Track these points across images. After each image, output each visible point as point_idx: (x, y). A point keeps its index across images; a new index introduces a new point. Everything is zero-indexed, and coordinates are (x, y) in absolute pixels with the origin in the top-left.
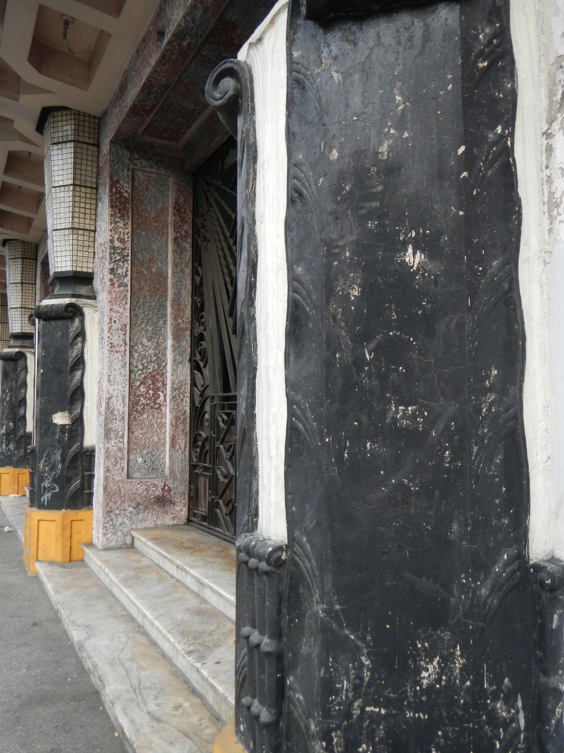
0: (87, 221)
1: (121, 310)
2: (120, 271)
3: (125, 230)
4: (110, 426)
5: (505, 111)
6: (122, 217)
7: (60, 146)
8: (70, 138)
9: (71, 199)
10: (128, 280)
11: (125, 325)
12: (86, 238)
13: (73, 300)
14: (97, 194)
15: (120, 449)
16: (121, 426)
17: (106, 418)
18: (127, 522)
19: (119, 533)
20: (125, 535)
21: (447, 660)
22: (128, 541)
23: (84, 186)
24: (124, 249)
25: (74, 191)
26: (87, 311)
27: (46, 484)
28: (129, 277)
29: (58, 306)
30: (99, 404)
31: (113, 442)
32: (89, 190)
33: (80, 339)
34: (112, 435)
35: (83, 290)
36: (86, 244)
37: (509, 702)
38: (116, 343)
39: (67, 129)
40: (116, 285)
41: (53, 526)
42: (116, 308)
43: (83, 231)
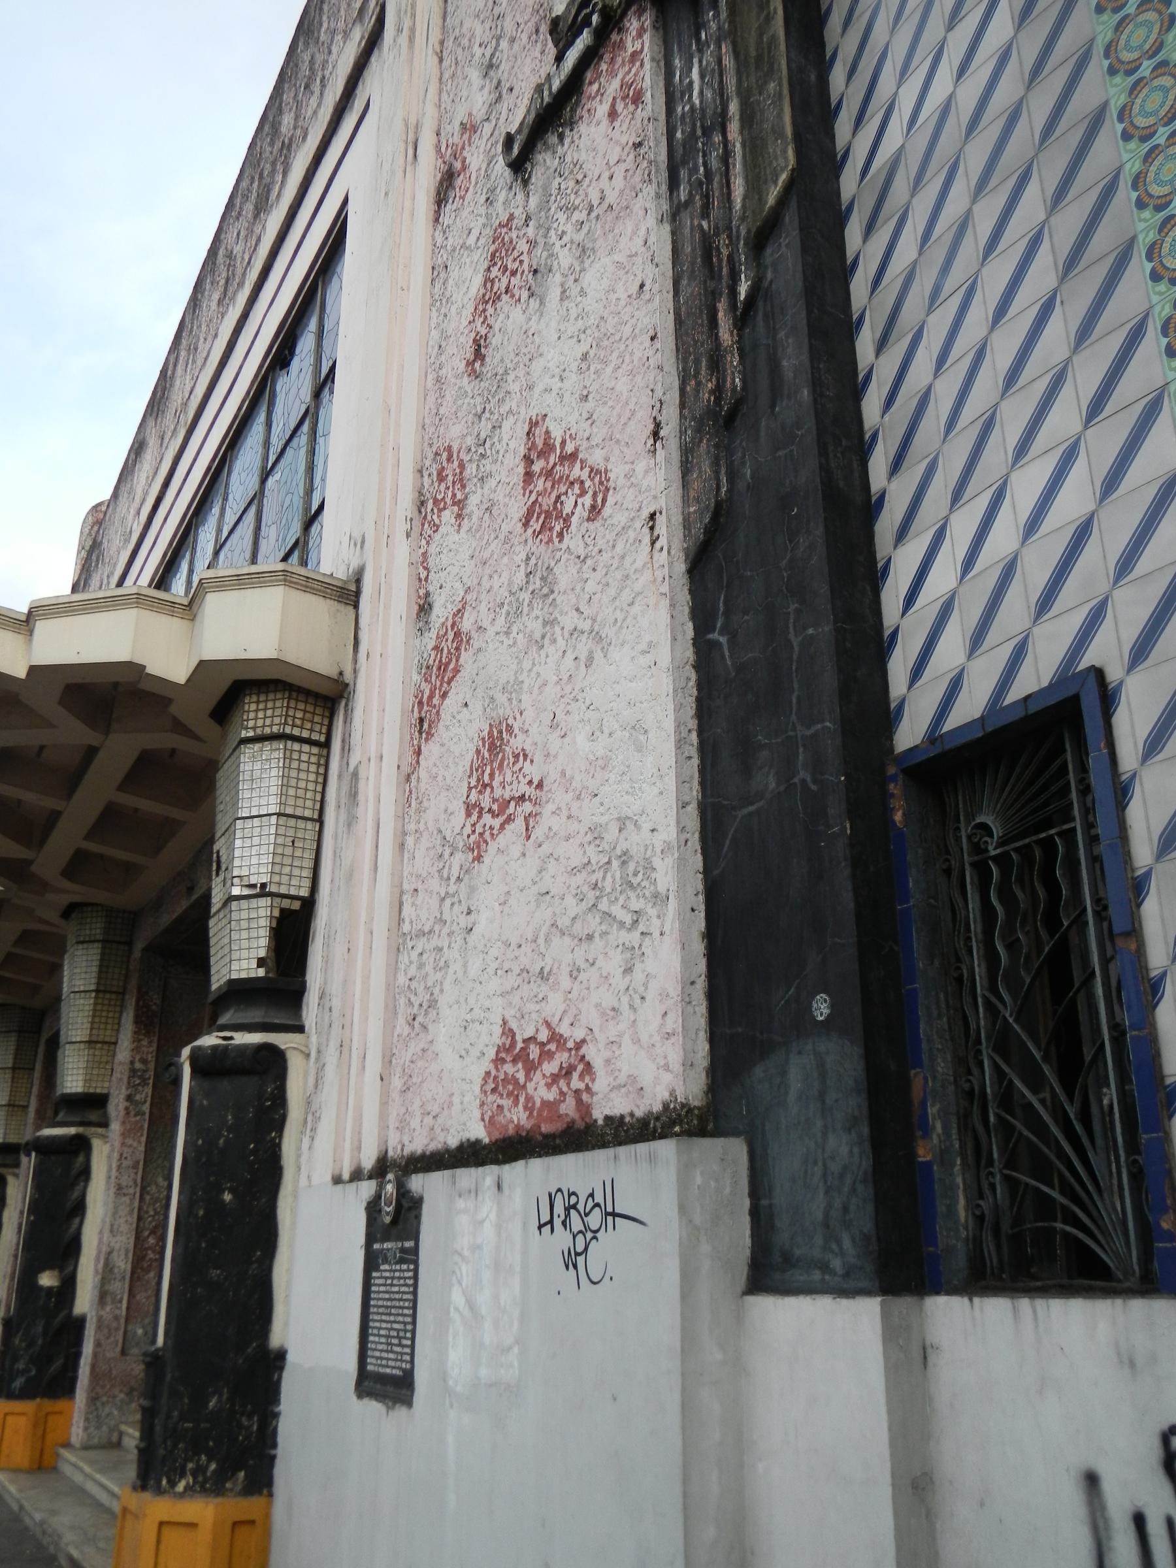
0: (108, 1033)
1: (135, 1144)
2: (138, 1097)
3: (149, 1049)
4: (107, 1287)
5: (280, 1124)
6: (148, 1033)
7: (85, 945)
8: (98, 937)
10: (146, 1108)
11: (138, 1162)
12: (104, 1052)
13: (81, 1130)
14: (123, 1000)
15: (116, 1318)
16: (120, 1288)
17: (103, 1278)
18: (116, 1413)
19: (104, 1428)
20: (111, 1430)
21: (221, 1396)
22: (115, 1438)
23: (107, 992)
24: (145, 1071)
25: (96, 998)
26: (96, 1144)
27: (21, 1365)
30: (97, 1259)
31: (108, 1308)
32: (114, 996)
33: (83, 1178)
34: (108, 1299)
35: (94, 1116)
36: (104, 1059)
37: (250, 1417)
38: (124, 1184)
39: (96, 928)
40: (132, 1113)
41: (22, 1421)
42: (129, 1141)
43: (100, 1044)
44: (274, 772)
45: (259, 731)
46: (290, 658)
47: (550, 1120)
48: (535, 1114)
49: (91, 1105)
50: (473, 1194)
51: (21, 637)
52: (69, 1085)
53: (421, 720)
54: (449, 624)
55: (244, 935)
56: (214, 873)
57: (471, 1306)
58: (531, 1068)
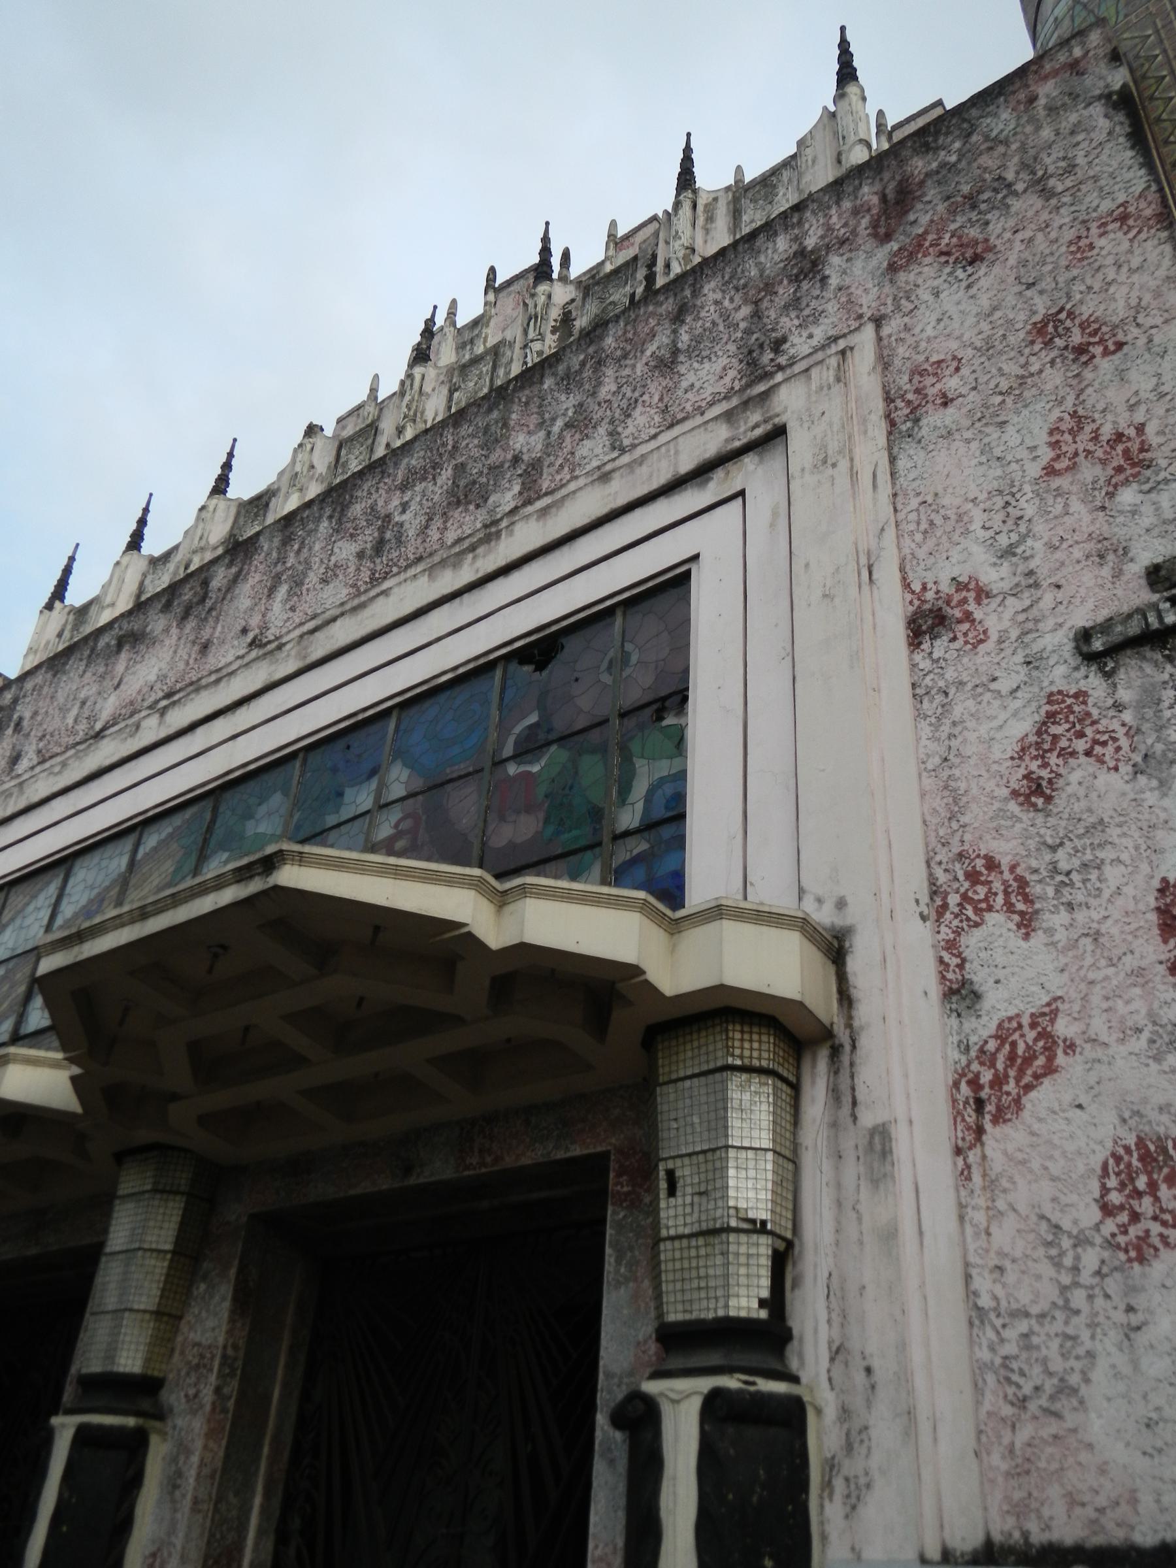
7: (165, 1196)
9: (164, 1271)
10: (231, 1404)
13: (141, 1421)
23: (188, 1260)
24: (235, 1359)
25: (172, 1260)
26: (154, 1439)
28: (232, 1401)
29: (122, 1429)
35: (146, 1404)
42: (211, 1444)
43: (168, 1316)
44: (764, 1107)
45: (747, 1062)
46: (807, 1002)
49: (141, 1392)
51: (492, 906)
52: (123, 1361)
53: (980, 1104)
54: (1026, 1021)
55: (743, 1271)
56: (663, 1194)
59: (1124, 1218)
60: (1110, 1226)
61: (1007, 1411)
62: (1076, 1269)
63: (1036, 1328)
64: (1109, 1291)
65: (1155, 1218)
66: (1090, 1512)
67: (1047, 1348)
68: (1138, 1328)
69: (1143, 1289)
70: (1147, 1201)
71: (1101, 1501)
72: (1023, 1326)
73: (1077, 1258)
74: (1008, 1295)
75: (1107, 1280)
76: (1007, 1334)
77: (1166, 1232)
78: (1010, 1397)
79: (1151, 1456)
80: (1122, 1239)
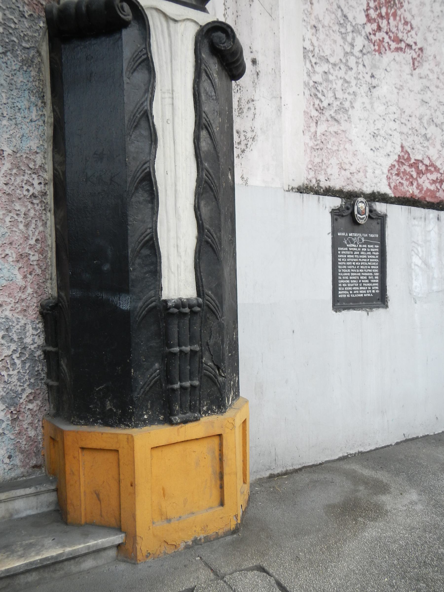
47: (432, 197)
48: (423, 192)
50: (423, 219)
57: (426, 263)
58: (420, 173)
59: (375, 26)
60: (369, 28)
61: (315, 113)
62: (352, 45)
63: (332, 71)
64: (366, 64)
65: (387, 33)
66: (347, 173)
67: (336, 83)
68: (375, 87)
69: (379, 68)
70: (385, 22)
71: (353, 169)
72: (326, 67)
73: (353, 39)
74: (319, 46)
75: (365, 56)
76: (317, 68)
77: (391, 43)
78: (316, 106)
79: (374, 151)
80: (372, 37)
